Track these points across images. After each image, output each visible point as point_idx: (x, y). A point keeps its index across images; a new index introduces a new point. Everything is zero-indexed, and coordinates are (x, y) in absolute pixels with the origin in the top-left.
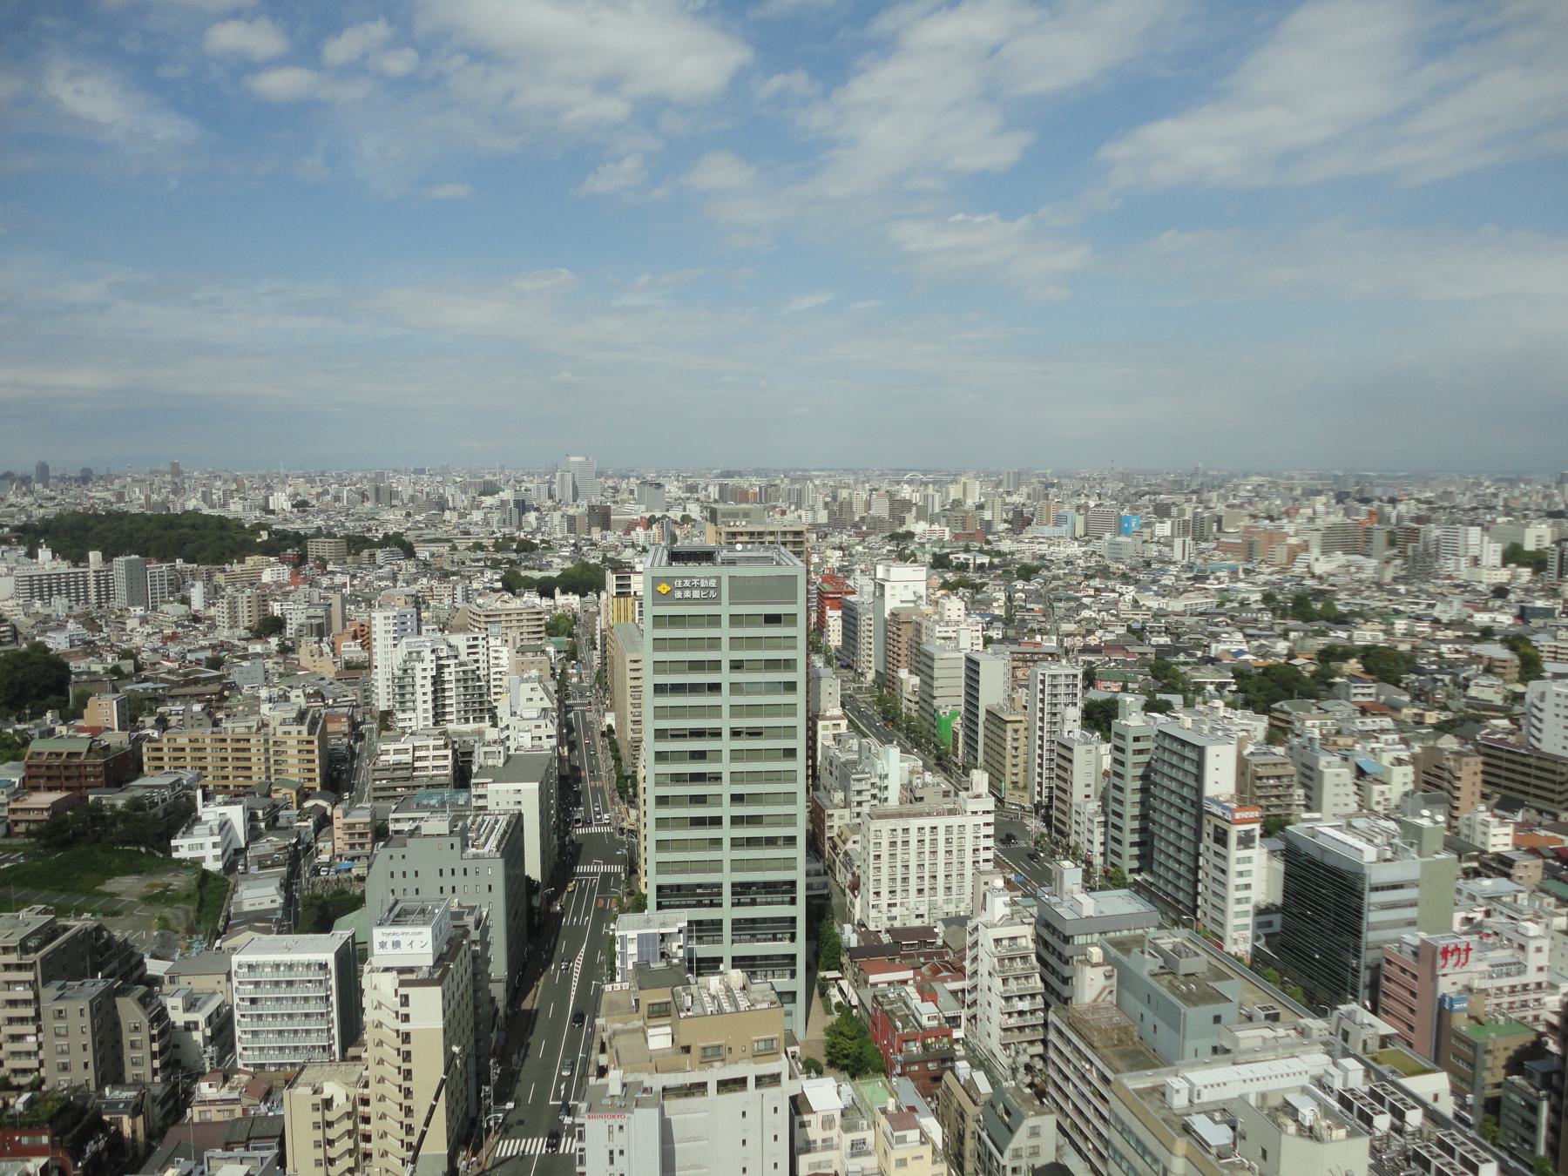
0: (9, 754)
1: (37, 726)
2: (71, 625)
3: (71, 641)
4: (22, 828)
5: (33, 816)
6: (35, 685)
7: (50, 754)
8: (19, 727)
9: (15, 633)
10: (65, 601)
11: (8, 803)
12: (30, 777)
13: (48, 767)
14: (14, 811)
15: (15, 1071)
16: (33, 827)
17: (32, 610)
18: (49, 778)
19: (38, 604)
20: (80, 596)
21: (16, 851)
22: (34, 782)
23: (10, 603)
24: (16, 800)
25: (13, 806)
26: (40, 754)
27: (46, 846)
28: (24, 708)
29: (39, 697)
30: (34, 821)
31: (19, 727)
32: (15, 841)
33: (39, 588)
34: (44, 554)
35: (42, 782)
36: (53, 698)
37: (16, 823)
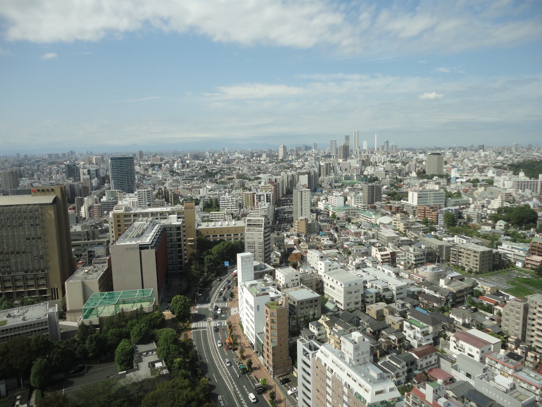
0: (521, 240)
1: (528, 233)
2: (535, 200)
3: (534, 205)
4: (529, 266)
5: (533, 263)
6: (526, 218)
7: (540, 243)
8: (523, 232)
9: (514, 201)
10: (530, 191)
11: (526, 257)
12: (532, 250)
13: (539, 248)
14: (527, 260)
15: (537, 346)
16: (534, 267)
17: (518, 193)
18: (538, 251)
19: (520, 191)
20: (534, 190)
21: (527, 273)
22: (533, 252)
23: (512, 190)
24: (528, 256)
25: (527, 258)
26: (536, 243)
27: (537, 274)
28: (522, 225)
29: (527, 223)
30: (534, 265)
31: (523, 232)
32: (527, 270)
33: (521, 185)
34: (522, 174)
35: (537, 252)
36: (532, 224)
37: (528, 264)
